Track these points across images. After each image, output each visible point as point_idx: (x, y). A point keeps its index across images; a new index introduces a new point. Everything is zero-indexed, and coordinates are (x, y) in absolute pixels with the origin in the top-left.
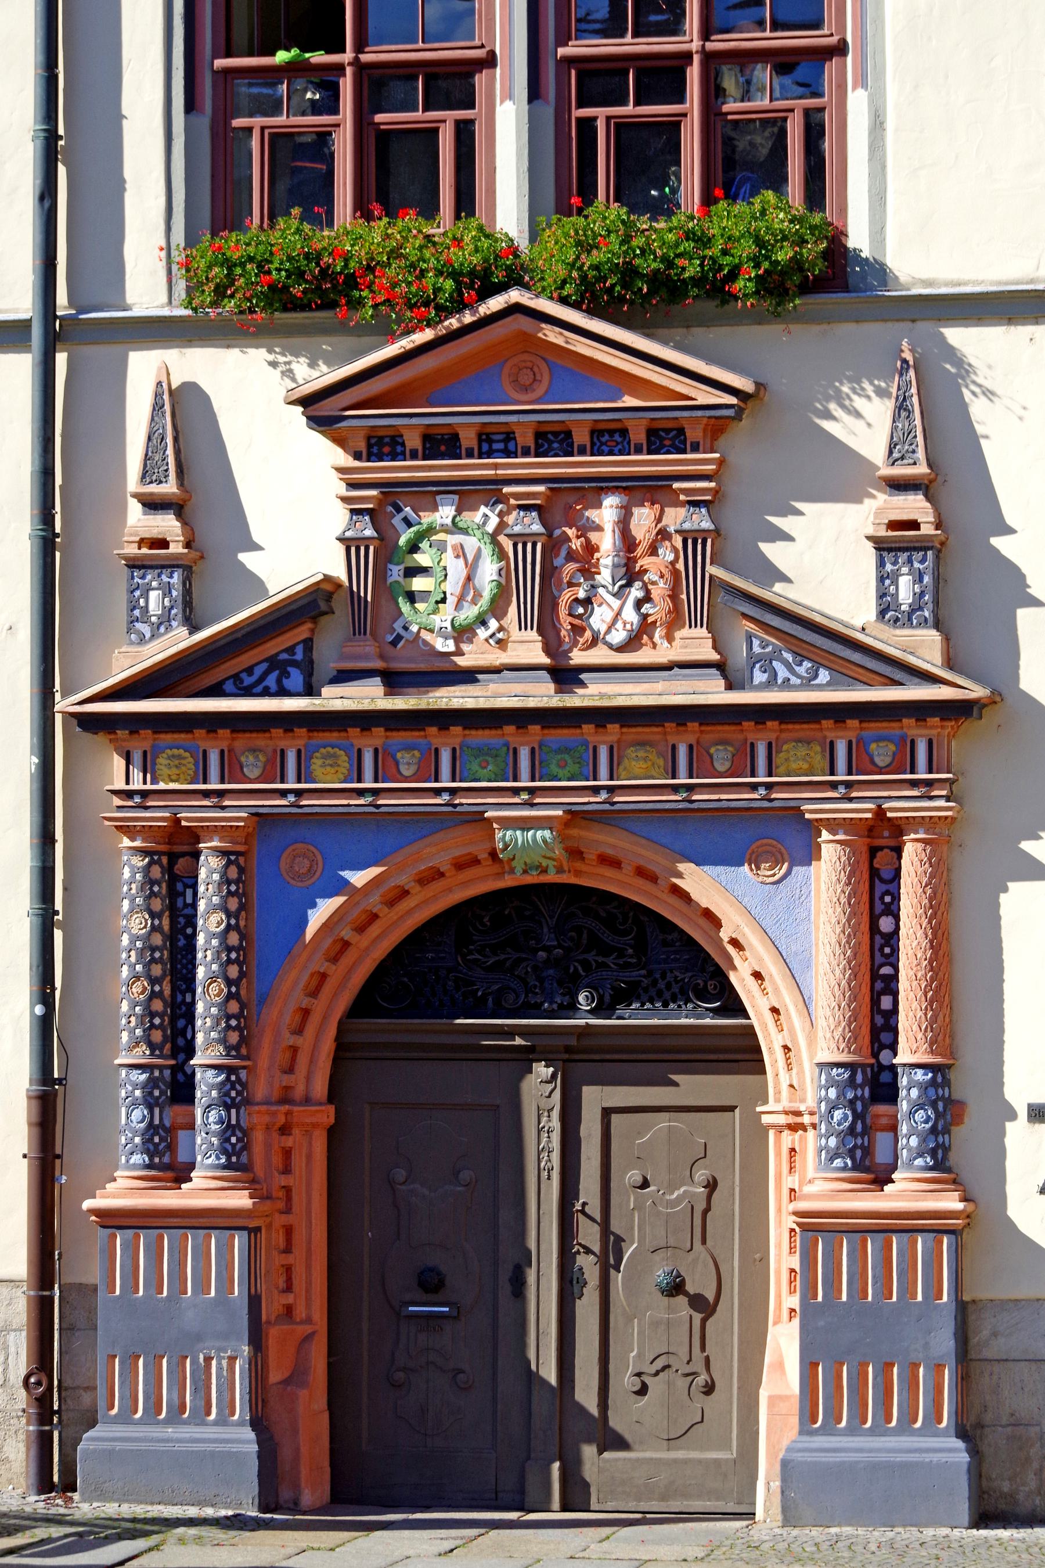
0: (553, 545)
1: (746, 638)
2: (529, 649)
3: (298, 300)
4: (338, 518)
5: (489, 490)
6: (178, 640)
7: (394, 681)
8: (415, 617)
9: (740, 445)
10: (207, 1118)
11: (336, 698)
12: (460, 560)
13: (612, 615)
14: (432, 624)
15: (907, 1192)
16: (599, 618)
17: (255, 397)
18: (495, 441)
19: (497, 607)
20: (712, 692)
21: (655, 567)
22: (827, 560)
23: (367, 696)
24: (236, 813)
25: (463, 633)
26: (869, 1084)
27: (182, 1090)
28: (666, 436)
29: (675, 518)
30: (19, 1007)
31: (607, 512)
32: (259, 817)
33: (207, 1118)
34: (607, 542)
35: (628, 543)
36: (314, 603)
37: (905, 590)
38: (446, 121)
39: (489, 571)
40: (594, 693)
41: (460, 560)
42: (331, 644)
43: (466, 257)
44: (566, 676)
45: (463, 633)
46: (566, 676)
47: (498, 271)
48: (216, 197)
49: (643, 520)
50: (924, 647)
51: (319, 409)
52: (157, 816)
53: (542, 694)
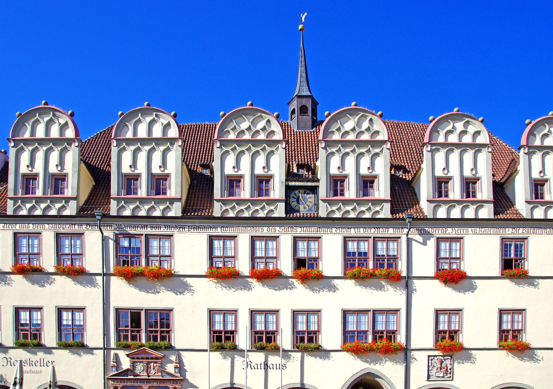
0: (148, 366)
1: (164, 374)
3: (126, 347)
4: (129, 364)
5: (142, 362)
6: (116, 372)
7: (134, 376)
8: (136, 371)
9: (163, 360)
11: (129, 377)
12: (139, 368)
13: (153, 372)
14: (138, 372)
16: (152, 372)
17: (122, 354)
18: (142, 358)
19: (143, 371)
20: (161, 378)
21: (156, 368)
22: (170, 368)
23: (132, 377)
24: (121, 386)
25: (140, 373)
28: (157, 358)
29: (158, 365)
31: (152, 364)
32: (123, 386)
34: (152, 366)
35: (154, 366)
36: (127, 370)
37: (177, 371)
38: (138, 334)
39: (142, 368)
40: (151, 378)
41: (139, 368)
42: (129, 373)
43: (140, 344)
44: (149, 376)
45: (140, 373)
46: (149, 376)
47: (142, 346)
48: (118, 339)
49: (155, 365)
50: (179, 375)
51: (128, 355)
52: (114, 386)
53: (147, 377)
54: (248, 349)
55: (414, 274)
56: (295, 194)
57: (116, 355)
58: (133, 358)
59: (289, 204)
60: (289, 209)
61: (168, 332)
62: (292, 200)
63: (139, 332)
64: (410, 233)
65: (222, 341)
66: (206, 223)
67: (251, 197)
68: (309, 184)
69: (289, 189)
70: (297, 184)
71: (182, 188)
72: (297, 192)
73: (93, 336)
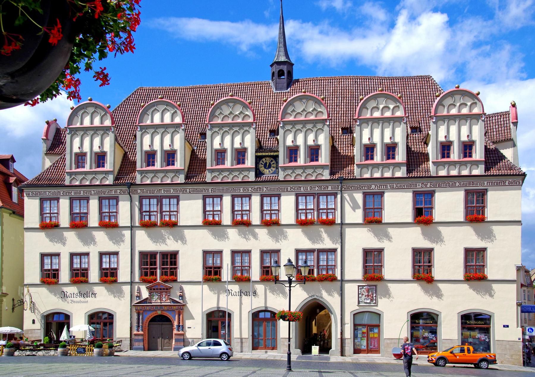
2: (159, 301)
6: (139, 301)
10: (140, 328)
15: (181, 332)
18: (157, 289)
26: (179, 326)
27: (139, 326)
30: (129, 322)
33: (140, 328)
36: (147, 299)
40: (162, 304)
42: (148, 301)
48: (141, 275)
54: (229, 280)
55: (347, 221)
56: (263, 161)
57: (139, 289)
58: (151, 290)
59: (259, 169)
60: (258, 173)
61: (176, 268)
62: (260, 165)
63: (156, 269)
64: (343, 189)
65: (212, 274)
66: (201, 187)
67: (232, 166)
68: (272, 154)
69: (258, 159)
70: (264, 154)
71: (185, 159)
72: (264, 160)
73: (124, 275)
